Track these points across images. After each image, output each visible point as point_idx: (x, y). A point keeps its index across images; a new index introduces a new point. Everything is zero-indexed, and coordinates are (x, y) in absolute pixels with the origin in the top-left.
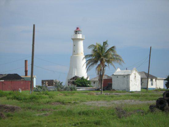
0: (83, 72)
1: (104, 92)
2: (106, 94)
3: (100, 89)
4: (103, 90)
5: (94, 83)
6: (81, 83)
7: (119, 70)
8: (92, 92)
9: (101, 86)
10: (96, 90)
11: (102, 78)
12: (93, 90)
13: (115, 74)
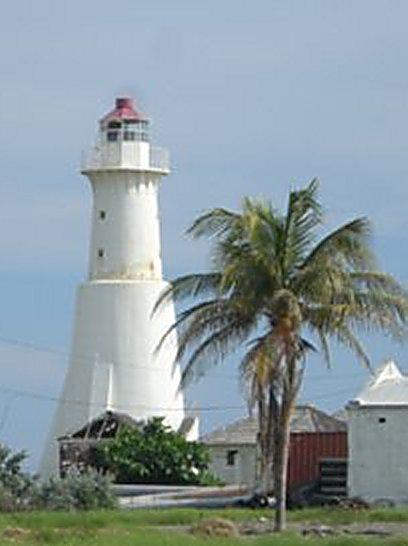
0: (157, 389)
1: (297, 520)
2: (305, 533)
3: (271, 500)
4: (289, 507)
5: (231, 462)
6: (144, 457)
7: (390, 373)
8: (216, 516)
9: (278, 481)
10: (241, 504)
11: (283, 424)
12: (223, 506)
13: (363, 403)
